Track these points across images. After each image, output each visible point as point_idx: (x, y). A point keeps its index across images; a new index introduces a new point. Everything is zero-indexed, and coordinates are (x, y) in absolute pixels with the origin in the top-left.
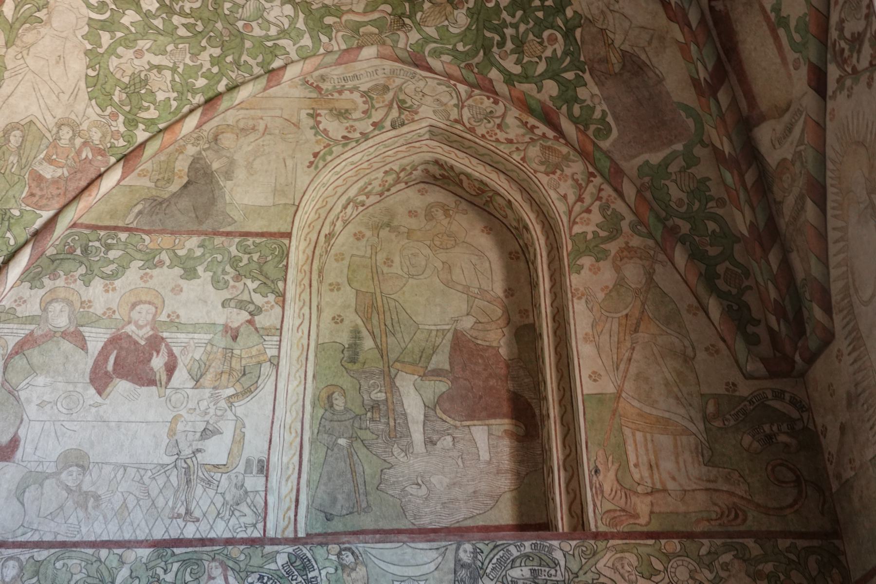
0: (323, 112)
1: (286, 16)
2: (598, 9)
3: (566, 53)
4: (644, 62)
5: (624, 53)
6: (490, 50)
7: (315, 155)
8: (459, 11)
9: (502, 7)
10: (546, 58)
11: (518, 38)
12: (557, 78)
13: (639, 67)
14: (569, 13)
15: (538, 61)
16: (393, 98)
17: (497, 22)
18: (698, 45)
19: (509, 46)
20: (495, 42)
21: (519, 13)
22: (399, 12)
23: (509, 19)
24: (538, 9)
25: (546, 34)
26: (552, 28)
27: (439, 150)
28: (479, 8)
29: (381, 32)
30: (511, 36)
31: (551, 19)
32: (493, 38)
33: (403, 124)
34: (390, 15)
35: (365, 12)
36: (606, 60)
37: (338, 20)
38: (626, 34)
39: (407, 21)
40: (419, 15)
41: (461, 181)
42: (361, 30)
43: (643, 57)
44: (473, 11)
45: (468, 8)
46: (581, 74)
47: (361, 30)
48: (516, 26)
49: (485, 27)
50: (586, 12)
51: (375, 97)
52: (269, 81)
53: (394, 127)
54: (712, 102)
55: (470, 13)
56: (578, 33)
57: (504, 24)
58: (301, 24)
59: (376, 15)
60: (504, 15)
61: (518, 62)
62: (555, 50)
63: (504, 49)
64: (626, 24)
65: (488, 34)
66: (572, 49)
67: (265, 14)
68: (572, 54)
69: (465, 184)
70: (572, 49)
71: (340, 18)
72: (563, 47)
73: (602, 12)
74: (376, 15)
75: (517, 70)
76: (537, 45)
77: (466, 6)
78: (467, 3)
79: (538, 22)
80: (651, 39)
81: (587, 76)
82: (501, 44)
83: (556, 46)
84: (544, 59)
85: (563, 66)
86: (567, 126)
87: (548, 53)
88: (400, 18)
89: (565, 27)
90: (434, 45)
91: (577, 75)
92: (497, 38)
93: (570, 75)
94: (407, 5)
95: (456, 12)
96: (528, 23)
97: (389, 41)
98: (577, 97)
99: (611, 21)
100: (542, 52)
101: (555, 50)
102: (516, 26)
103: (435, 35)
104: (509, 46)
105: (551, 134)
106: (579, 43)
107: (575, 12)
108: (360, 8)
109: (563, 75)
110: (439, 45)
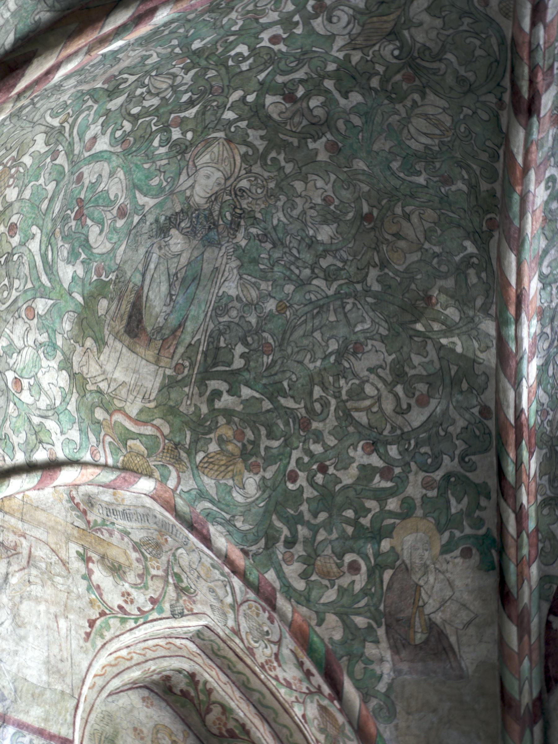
0: (95, 557)
1: (60, 388)
2: (421, 558)
3: (365, 592)
4: (451, 646)
5: (431, 626)
6: (274, 544)
7: (92, 623)
8: (252, 475)
9: (305, 496)
10: (340, 587)
11: (313, 545)
12: (345, 617)
13: (444, 649)
14: (385, 545)
15: (329, 585)
16: (168, 567)
17: (292, 512)
18: (530, 660)
19: (299, 550)
20: (282, 538)
21: (323, 516)
22: (177, 440)
23: (307, 516)
24: (348, 521)
25: (348, 558)
26: (359, 553)
27: (200, 661)
28: (277, 483)
29: (149, 456)
30: (304, 537)
31: (361, 542)
32: (279, 531)
33: (182, 615)
34: (165, 437)
35: (137, 421)
36: (409, 623)
37: (108, 417)
38: (443, 603)
39: (184, 455)
40: (200, 456)
41: (209, 711)
42: (130, 443)
43: (453, 639)
44: (269, 483)
45: (263, 478)
46: (375, 626)
47: (130, 443)
48: (315, 530)
49: (276, 511)
50: (405, 555)
51: (148, 556)
52: (39, 482)
53: (174, 616)
54: (528, 732)
55: (263, 486)
56: (387, 575)
57: (299, 519)
58: (72, 407)
59: (148, 430)
60: (304, 508)
61: (304, 575)
62: (353, 582)
63: (291, 550)
64: (449, 593)
65: (278, 524)
66: (373, 590)
67: (40, 375)
68: (372, 596)
69: (211, 718)
70: (373, 590)
71: (111, 415)
72: (364, 584)
73: (426, 566)
74: (148, 430)
75: (300, 585)
76: (334, 566)
77: (262, 473)
78: (264, 470)
79: (343, 537)
80: (469, 623)
81: (381, 632)
82: (290, 543)
83: (357, 578)
84: (336, 587)
85: (356, 606)
86: (349, 687)
87: (345, 581)
88: (176, 448)
89: (375, 561)
90: (208, 505)
91: (370, 627)
92: (286, 532)
93: (361, 621)
94: (188, 434)
95: (246, 474)
96: (330, 532)
97: (157, 474)
98: (362, 654)
99: (431, 579)
100: (337, 579)
101: (353, 582)
102: (315, 530)
103: (213, 492)
104: (299, 550)
105: (326, 690)
106: (385, 587)
107: (393, 548)
108: (134, 411)
109: (353, 617)
110: (214, 508)
